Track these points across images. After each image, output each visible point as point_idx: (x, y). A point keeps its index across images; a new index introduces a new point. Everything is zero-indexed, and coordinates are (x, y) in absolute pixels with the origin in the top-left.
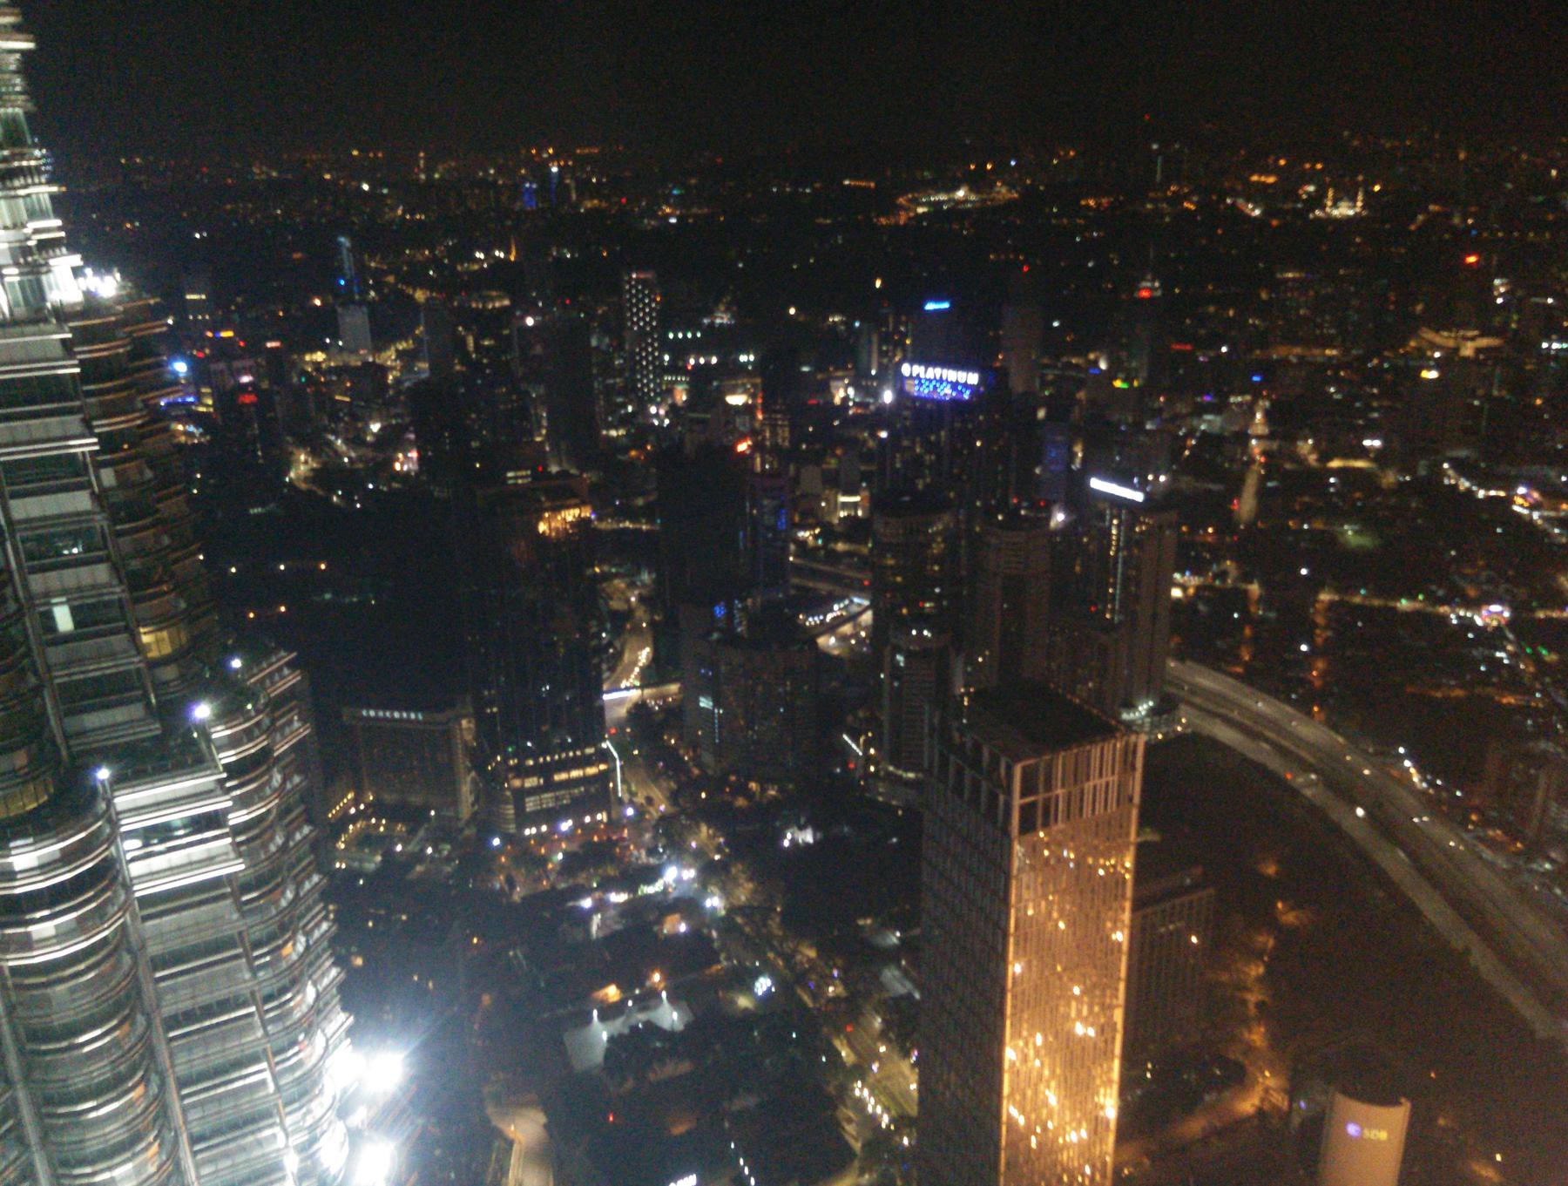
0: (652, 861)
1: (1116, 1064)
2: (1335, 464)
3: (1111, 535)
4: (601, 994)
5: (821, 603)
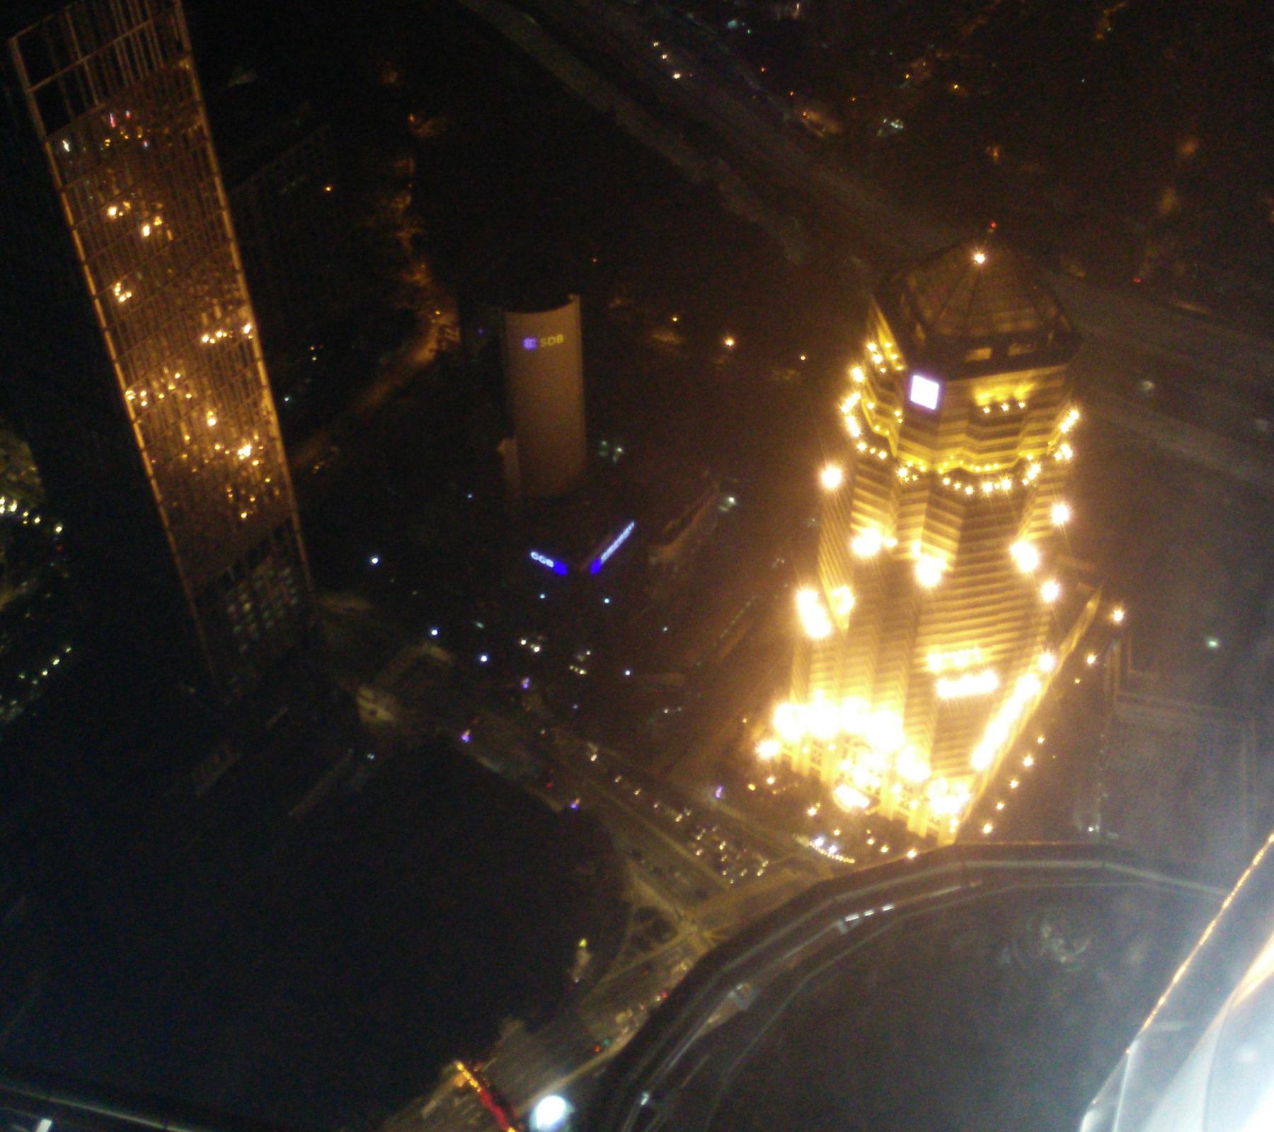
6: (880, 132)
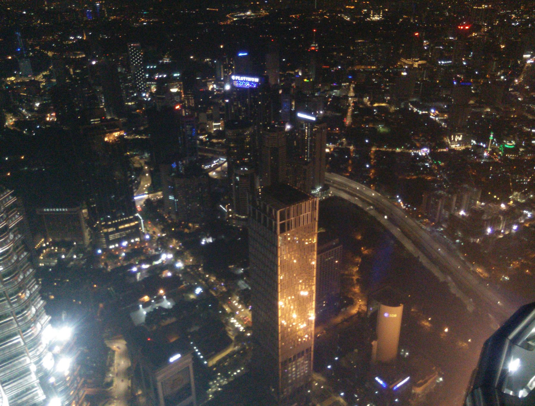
1: (314, 303)
2: (376, 105)
4: (142, 299)
5: (209, 161)
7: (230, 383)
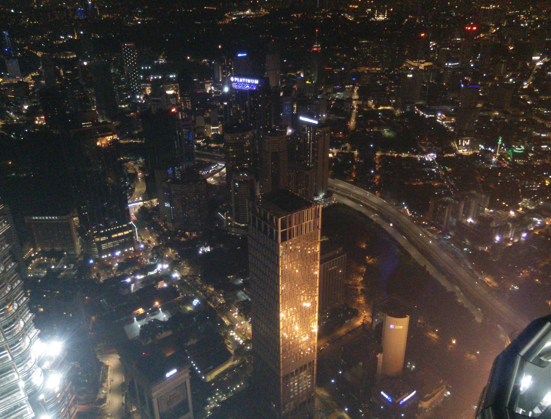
0: (152, 263)
1: (317, 314)
2: (381, 108)
3: (308, 136)
4: (137, 311)
5: (207, 166)
6: (510, 289)
7: (229, 399)
